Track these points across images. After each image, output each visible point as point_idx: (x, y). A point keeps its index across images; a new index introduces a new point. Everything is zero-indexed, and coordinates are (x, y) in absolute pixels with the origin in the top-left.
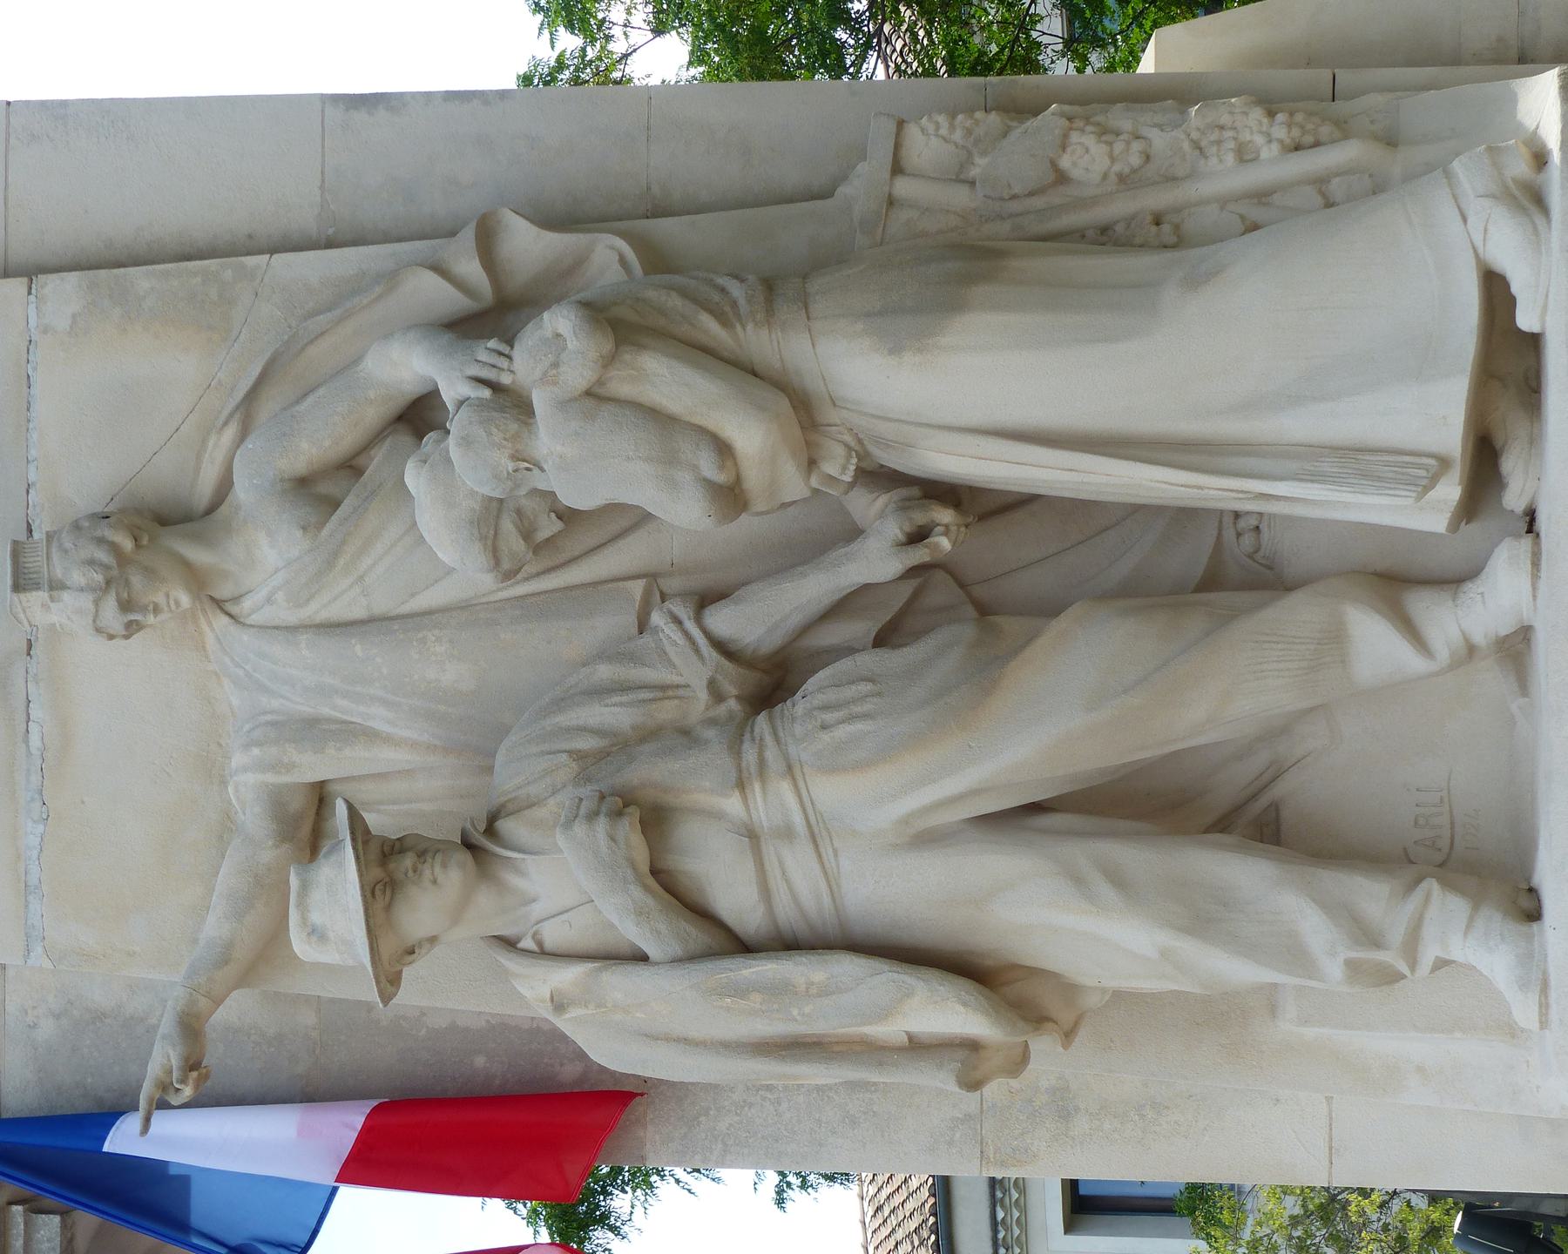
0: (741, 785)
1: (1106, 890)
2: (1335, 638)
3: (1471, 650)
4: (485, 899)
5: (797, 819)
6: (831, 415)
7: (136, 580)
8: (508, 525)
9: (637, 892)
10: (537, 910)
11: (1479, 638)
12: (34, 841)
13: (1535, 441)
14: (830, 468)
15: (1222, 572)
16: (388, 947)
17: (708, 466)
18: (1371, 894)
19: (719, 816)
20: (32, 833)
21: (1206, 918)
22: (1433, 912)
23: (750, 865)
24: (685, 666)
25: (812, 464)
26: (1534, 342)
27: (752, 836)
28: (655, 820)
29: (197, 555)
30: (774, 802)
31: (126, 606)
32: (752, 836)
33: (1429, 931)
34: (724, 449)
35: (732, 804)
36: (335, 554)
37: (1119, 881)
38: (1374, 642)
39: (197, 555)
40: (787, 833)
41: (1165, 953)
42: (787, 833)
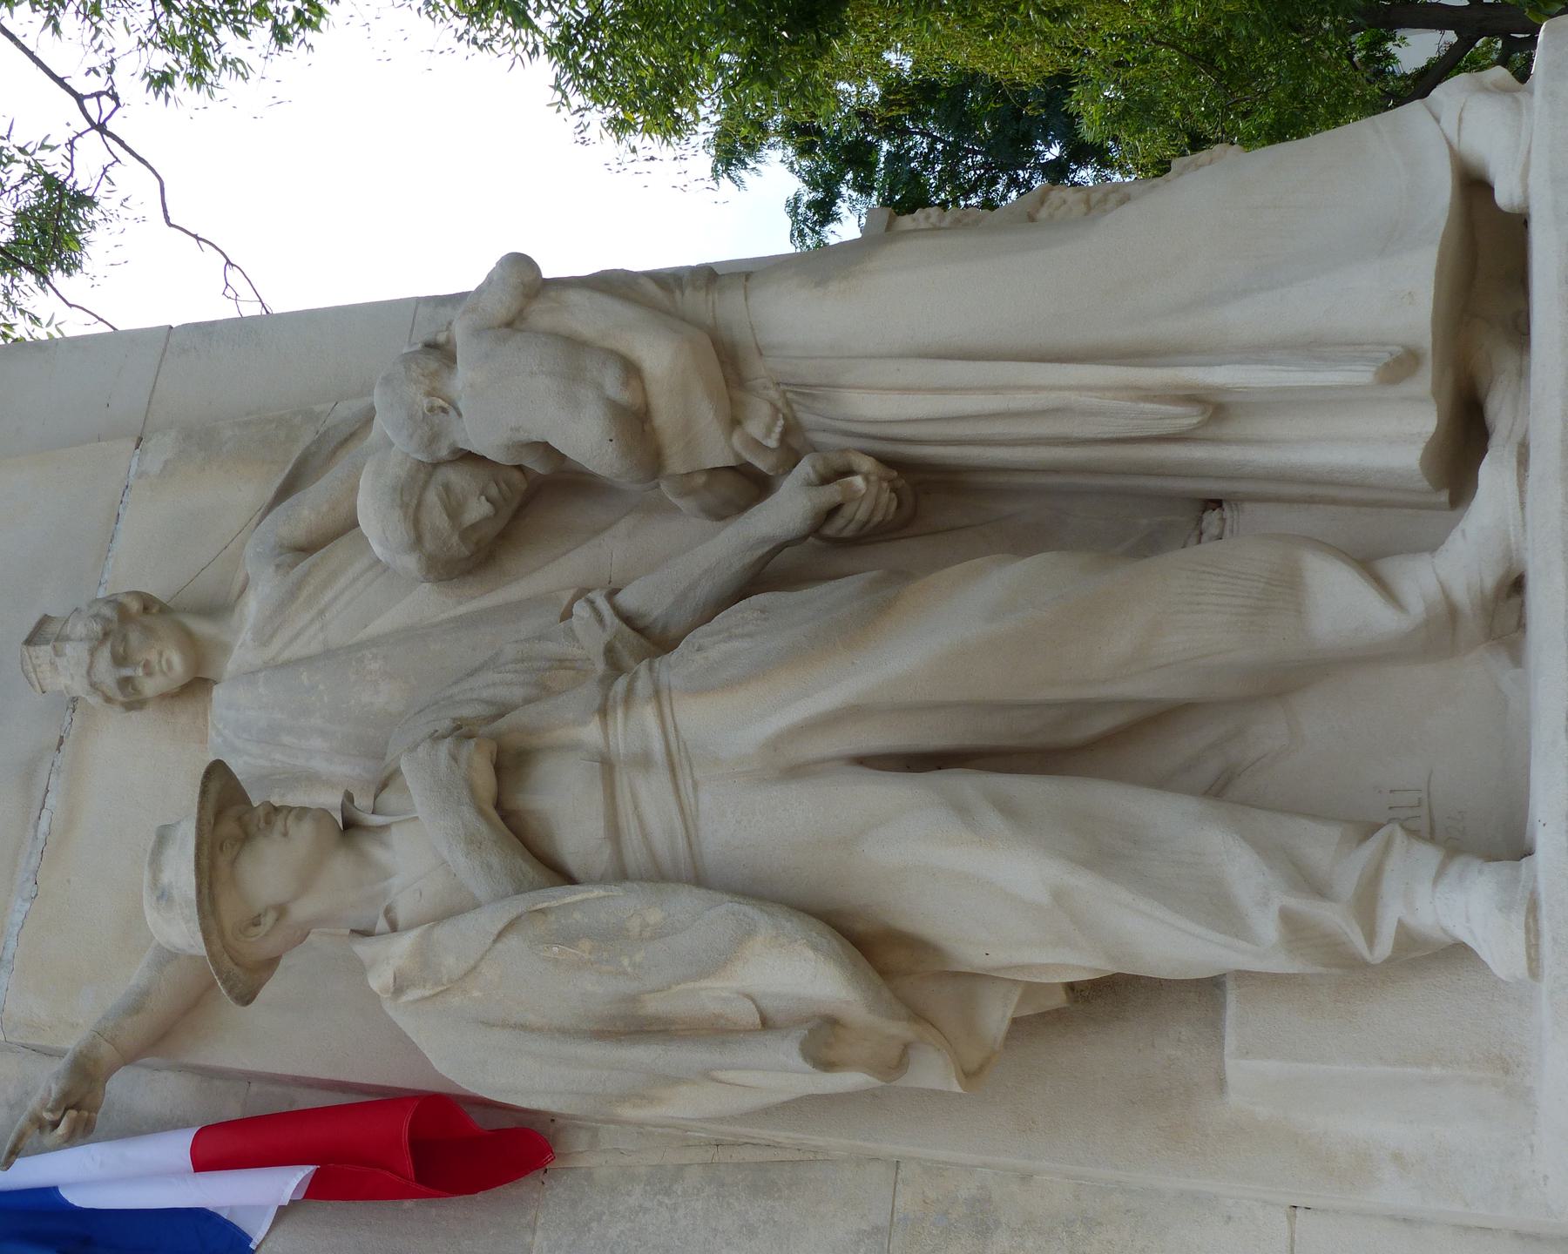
0: (604, 712)
1: (994, 820)
2: (1290, 584)
3: (1452, 613)
4: (340, 866)
5: (657, 746)
6: (759, 370)
7: (134, 637)
8: (432, 497)
9: (469, 813)
10: (396, 882)
11: (1461, 596)
12: (19, 918)
13: (1523, 373)
14: (755, 428)
15: (1156, 508)
16: (230, 912)
17: (611, 383)
18: (1319, 845)
19: (575, 747)
20: (19, 908)
21: (1111, 854)
22: (1394, 864)
23: (598, 796)
24: (589, 636)
25: (735, 422)
26: (1518, 224)
27: (607, 765)
28: (512, 762)
29: (202, 627)
30: (638, 727)
31: (120, 660)
32: (607, 765)
33: (1391, 886)
34: (631, 370)
35: (591, 733)
36: (299, 585)
37: (1008, 809)
38: (1340, 602)
39: (202, 627)
40: (644, 761)
41: (1059, 896)
42: (644, 761)
